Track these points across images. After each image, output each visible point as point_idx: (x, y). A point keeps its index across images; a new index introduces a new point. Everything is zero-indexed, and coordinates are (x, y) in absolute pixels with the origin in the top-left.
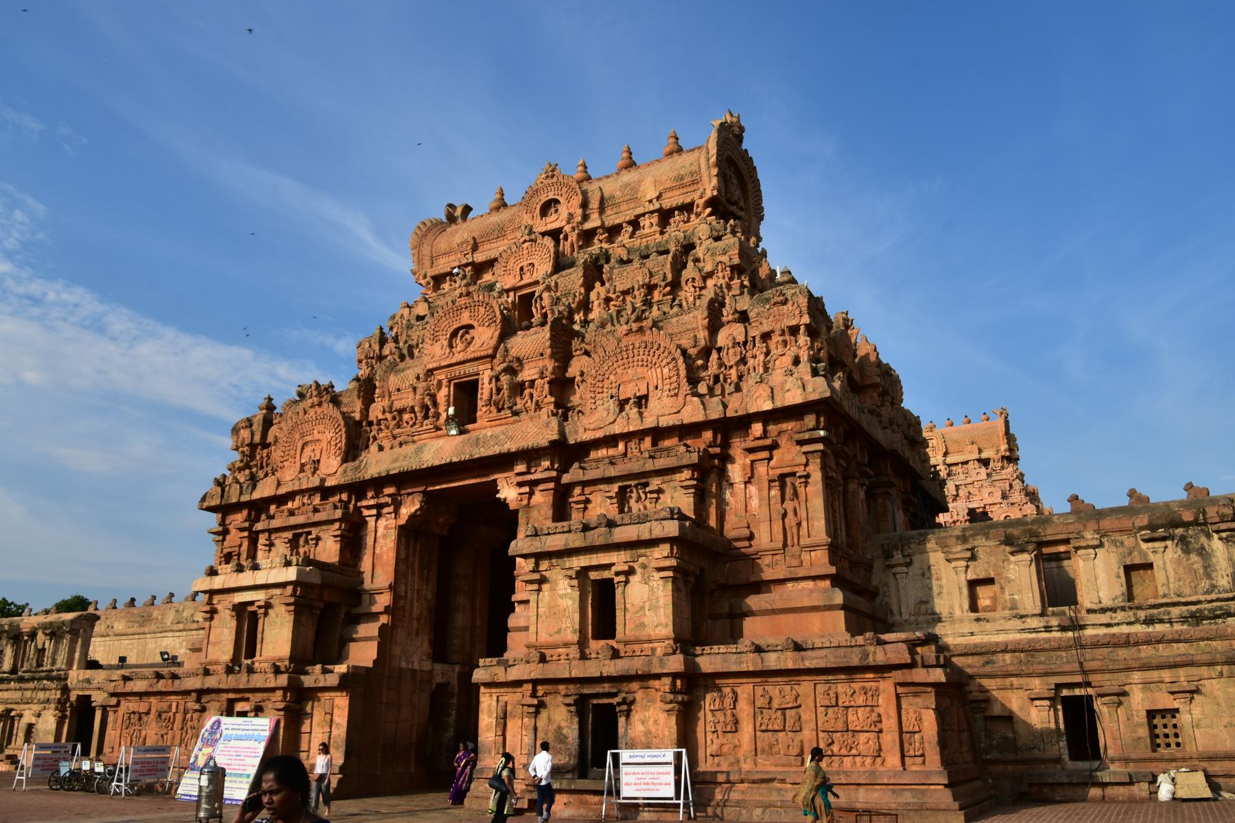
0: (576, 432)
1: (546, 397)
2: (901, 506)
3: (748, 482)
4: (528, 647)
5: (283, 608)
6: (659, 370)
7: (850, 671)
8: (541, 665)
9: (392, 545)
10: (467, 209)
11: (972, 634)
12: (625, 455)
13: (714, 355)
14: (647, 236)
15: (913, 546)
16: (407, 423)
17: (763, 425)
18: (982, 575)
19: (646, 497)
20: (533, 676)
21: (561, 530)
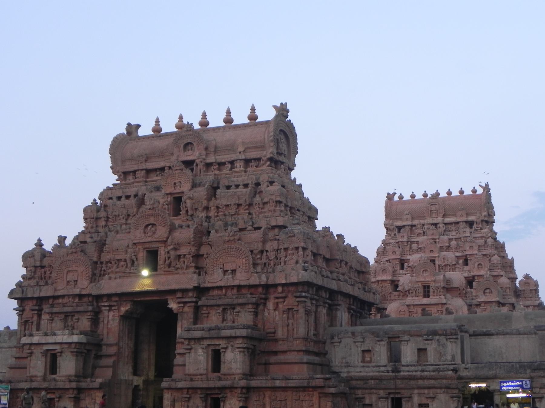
0: (205, 283)
1: (191, 263)
2: (347, 310)
3: (275, 310)
4: (186, 375)
5: (70, 353)
6: (241, 260)
7: (304, 389)
8: (191, 382)
9: (117, 324)
10: (138, 126)
11: (361, 372)
12: (225, 295)
13: (265, 252)
14: (238, 172)
15: (342, 335)
16: (122, 266)
17: (282, 288)
18: (366, 348)
19: (234, 313)
20: (188, 386)
21: (199, 329)
